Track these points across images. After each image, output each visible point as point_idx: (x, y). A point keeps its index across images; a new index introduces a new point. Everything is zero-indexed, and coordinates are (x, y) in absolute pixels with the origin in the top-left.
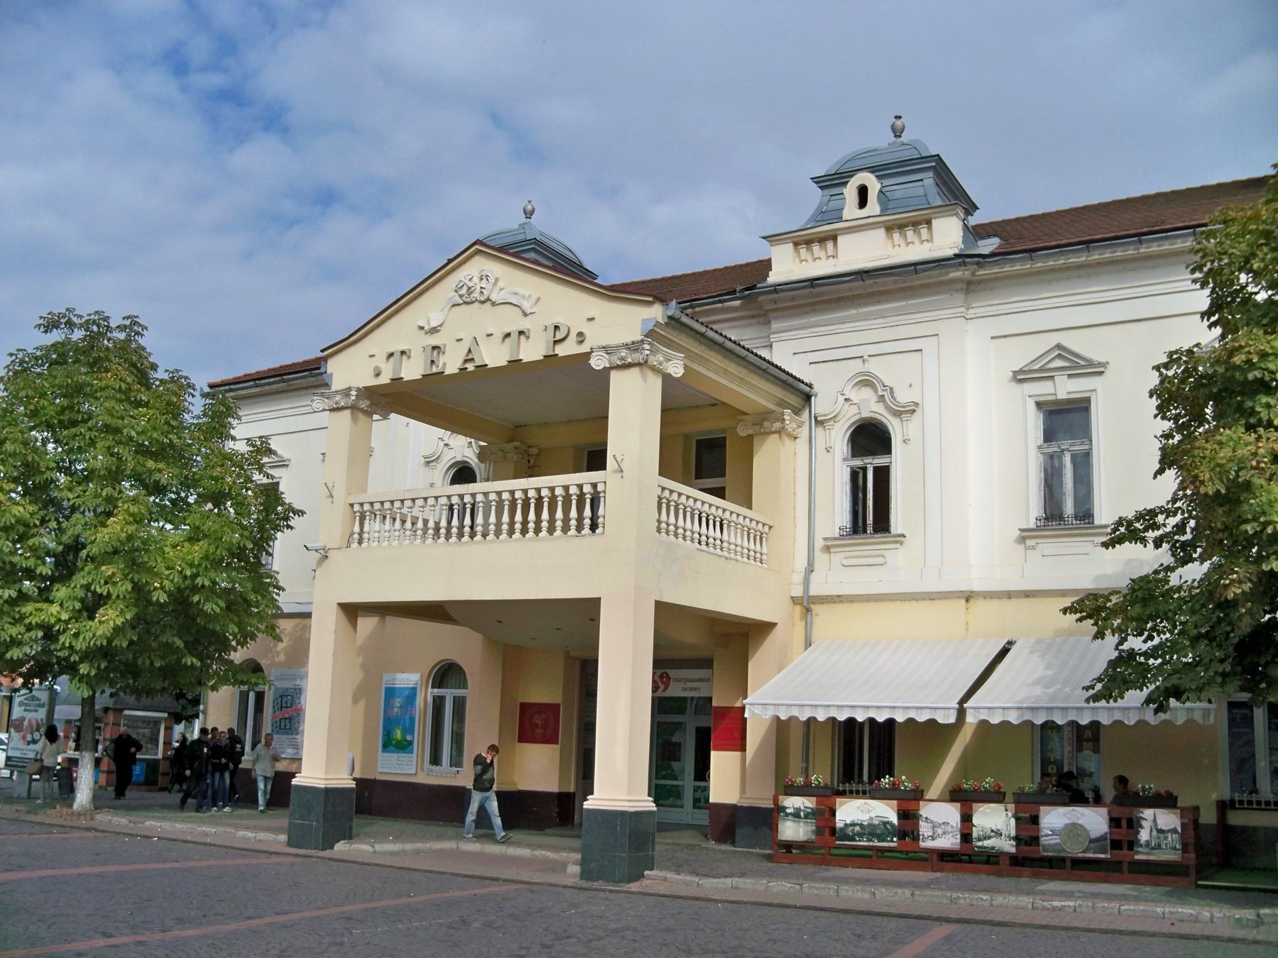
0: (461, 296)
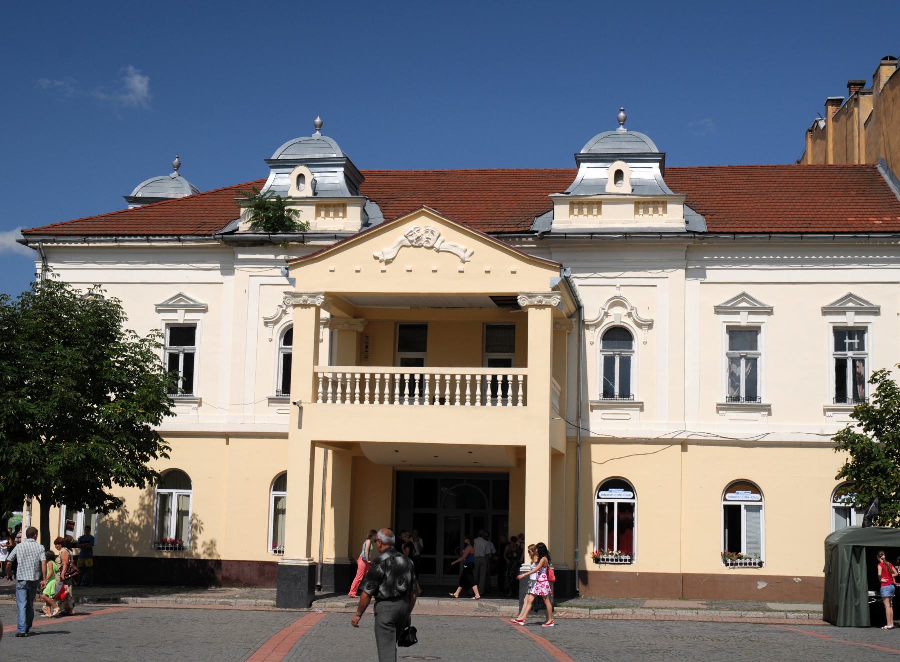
0: (411, 242)
